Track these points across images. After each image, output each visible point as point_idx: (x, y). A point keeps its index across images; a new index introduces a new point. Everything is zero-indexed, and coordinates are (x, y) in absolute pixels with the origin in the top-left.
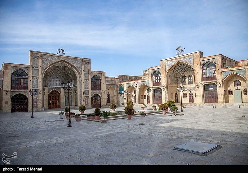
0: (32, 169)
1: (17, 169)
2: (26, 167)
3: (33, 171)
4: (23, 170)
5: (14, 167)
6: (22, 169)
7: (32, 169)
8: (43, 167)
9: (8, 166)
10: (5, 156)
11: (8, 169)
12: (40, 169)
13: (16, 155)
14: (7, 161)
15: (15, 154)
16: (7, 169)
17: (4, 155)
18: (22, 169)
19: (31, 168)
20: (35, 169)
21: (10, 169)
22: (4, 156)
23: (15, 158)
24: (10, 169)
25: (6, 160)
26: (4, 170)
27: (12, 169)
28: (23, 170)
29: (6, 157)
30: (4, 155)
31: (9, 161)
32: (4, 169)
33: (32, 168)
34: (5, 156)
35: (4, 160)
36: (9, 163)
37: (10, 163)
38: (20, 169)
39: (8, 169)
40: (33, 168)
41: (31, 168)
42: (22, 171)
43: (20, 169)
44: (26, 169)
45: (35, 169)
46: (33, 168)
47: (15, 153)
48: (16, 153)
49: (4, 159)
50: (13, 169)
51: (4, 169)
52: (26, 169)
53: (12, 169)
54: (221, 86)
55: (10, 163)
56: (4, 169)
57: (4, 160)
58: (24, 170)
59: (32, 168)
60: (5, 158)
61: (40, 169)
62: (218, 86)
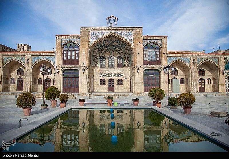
0: (29, 155)
1: (16, 155)
2: (24, 153)
3: (31, 157)
4: (21, 156)
6: (21, 156)
7: (29, 155)
8: (40, 153)
9: (7, 153)
10: (4, 143)
11: (8, 156)
12: (37, 156)
13: (15, 143)
14: (7, 148)
15: (14, 142)
16: (7, 156)
17: (3, 142)
18: (21, 156)
19: (28, 154)
20: (32, 156)
21: (9, 156)
22: (3, 143)
23: (14, 145)
24: (9, 156)
25: (6, 147)
26: (3, 156)
27: (11, 156)
28: (21, 156)
30: (3, 142)
31: (8, 148)
32: (4, 156)
33: (29, 155)
34: (4, 143)
35: (4, 147)
36: (8, 150)
37: (9, 150)
38: (19, 156)
39: (8, 156)
40: (30, 154)
41: (28, 154)
42: (20, 158)
43: (19, 156)
44: (24, 156)
45: (32, 156)
46: (30, 154)
47: (13, 141)
48: (15, 141)
49: (3, 146)
50: (12, 156)
51: (4, 156)
52: (24, 156)
53: (11, 156)
54: (60, 73)
55: (9, 150)
56: (4, 156)
58: (22, 156)
59: (29, 155)
61: (37, 156)
62: (81, 71)
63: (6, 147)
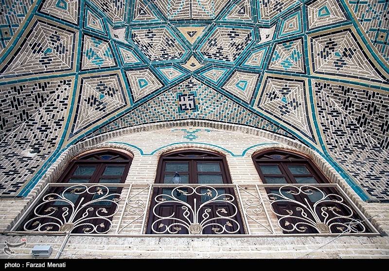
1: (27, 265)
2: (41, 261)
3: (52, 268)
4: (36, 266)
5: (22, 261)
6: (35, 265)
8: (68, 261)
10: (8, 245)
11: (13, 265)
12: (63, 265)
16: (11, 265)
18: (35, 265)
19: (48, 263)
20: (54, 265)
21: (16, 265)
24: (16, 265)
25: (9, 251)
26: (6, 267)
27: (18, 265)
28: (36, 266)
29: (9, 246)
33: (50, 263)
34: (8, 245)
35: (6, 251)
38: (32, 265)
39: (13, 265)
40: (51, 263)
41: (48, 263)
42: (34, 268)
43: (32, 265)
44: (40, 265)
45: (54, 265)
46: (51, 263)
50: (21, 265)
51: (6, 265)
52: (40, 265)
53: (18, 265)
56: (7, 265)
57: (6, 251)
58: (38, 266)
59: (50, 263)
60: (7, 247)
61: (63, 265)
63: (9, 251)
